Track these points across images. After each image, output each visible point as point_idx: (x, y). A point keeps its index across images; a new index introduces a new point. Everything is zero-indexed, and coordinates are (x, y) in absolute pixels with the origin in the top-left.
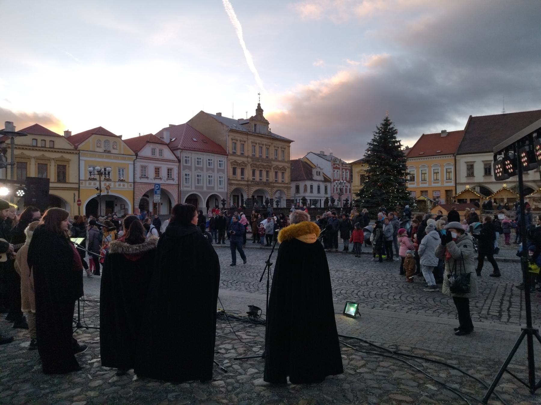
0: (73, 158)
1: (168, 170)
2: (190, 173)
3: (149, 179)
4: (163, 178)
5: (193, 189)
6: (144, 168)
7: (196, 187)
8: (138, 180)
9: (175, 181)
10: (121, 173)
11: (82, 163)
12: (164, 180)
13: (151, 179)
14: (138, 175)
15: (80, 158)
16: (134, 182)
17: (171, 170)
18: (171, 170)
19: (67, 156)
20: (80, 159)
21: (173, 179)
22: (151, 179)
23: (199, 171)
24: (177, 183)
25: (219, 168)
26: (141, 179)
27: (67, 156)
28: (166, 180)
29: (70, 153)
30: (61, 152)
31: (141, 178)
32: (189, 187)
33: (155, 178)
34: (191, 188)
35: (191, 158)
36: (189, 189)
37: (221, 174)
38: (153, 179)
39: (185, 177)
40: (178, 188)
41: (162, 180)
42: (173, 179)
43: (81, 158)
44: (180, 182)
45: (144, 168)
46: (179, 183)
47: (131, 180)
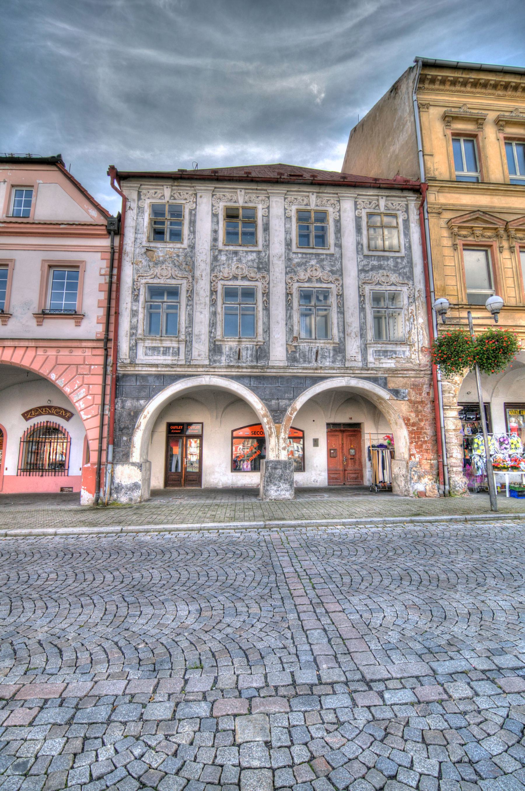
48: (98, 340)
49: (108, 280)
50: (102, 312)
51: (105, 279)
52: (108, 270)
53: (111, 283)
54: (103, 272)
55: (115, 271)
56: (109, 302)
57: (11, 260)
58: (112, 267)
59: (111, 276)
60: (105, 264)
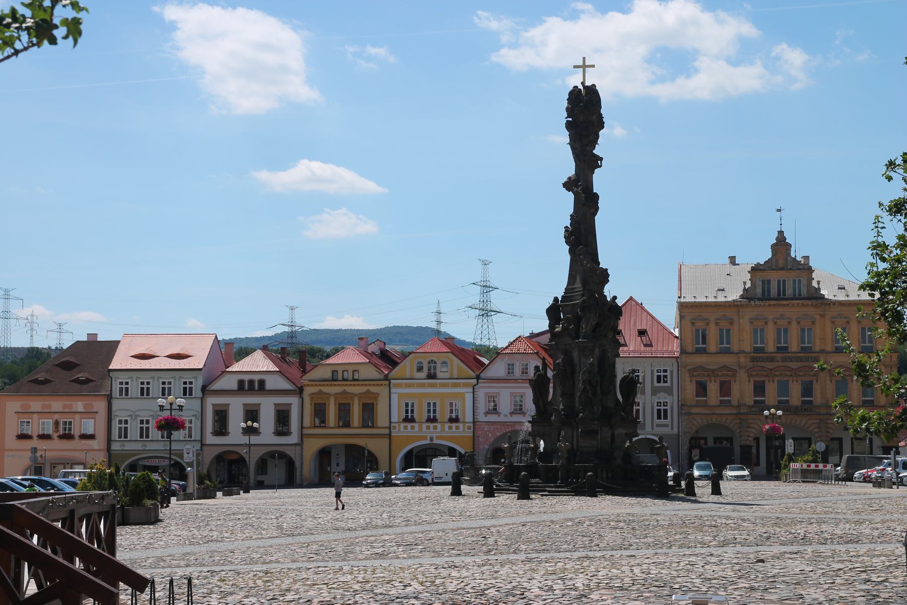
0: (382, 391)
3: (502, 416)
4: (529, 413)
6: (492, 399)
8: (481, 417)
11: (395, 398)
14: (481, 409)
16: (474, 422)
20: (391, 392)
22: (506, 416)
25: (656, 384)
26: (486, 416)
27: (374, 389)
29: (382, 384)
33: (512, 413)
37: (662, 397)
38: (509, 416)
41: (527, 415)
43: (393, 390)
45: (492, 399)
47: (469, 418)
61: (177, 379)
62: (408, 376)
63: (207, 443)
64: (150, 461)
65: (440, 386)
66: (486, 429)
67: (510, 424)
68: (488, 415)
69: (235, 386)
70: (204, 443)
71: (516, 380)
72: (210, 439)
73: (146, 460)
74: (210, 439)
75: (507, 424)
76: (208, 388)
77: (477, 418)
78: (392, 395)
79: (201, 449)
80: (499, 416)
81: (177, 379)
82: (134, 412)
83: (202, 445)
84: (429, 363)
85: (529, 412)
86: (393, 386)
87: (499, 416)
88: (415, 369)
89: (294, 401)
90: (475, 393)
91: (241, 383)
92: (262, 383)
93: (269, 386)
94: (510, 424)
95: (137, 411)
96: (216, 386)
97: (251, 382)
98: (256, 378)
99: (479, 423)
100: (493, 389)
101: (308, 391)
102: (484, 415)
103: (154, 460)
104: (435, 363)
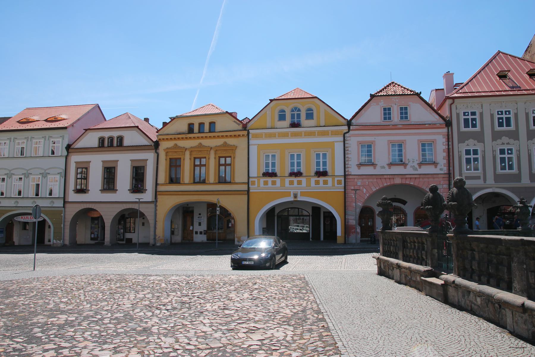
0: (241, 143)
1: (423, 145)
2: (479, 147)
3: (378, 167)
4: (411, 164)
5: (490, 180)
6: (369, 148)
7: (498, 178)
8: (353, 170)
9: (439, 167)
10: (321, 160)
11: (254, 150)
12: (413, 167)
13: (383, 167)
15: (250, 141)
16: (345, 176)
17: (430, 145)
18: (430, 145)
19: (231, 141)
21: (435, 164)
22: (383, 167)
23: (505, 139)
24: (445, 170)
27: (231, 141)
28: (417, 166)
29: (239, 136)
30: (222, 136)
31: (360, 165)
32: (478, 178)
34: (485, 180)
35: (481, 114)
36: (479, 183)
38: (387, 167)
39: (464, 157)
40: (447, 182)
41: (408, 167)
42: (435, 164)
43: (251, 142)
44: (451, 168)
46: (449, 170)
47: (339, 170)
48: (445, 174)
49: (447, 148)
50: (445, 161)
51: (446, 147)
52: (447, 143)
53: (449, 149)
54: (444, 144)
55: (450, 143)
56: (449, 157)
57: (405, 140)
58: (448, 141)
59: (448, 145)
60: (444, 140)
61: (47, 139)
62: (269, 125)
63: (69, 201)
64: (24, 218)
65: (305, 135)
66: (359, 184)
67: (389, 177)
68: (362, 168)
69: (95, 144)
70: (66, 200)
71: (395, 127)
72: (73, 197)
73: (20, 217)
74: (73, 197)
75: (385, 177)
76: (72, 147)
77: (350, 170)
78: (250, 147)
79: (64, 207)
80: (375, 168)
81: (47, 139)
82: (10, 171)
83: (65, 202)
84: (292, 111)
85: (411, 162)
86: (253, 137)
87: (375, 168)
88: (277, 117)
89: (150, 156)
90: (346, 142)
91: (102, 140)
92: (121, 139)
93: (126, 143)
94: (389, 177)
95: (12, 170)
96: (80, 144)
97: (111, 139)
98: (115, 134)
99: (351, 177)
100: (367, 137)
101: (164, 145)
102: (356, 167)
103: (27, 216)
104: (299, 110)
